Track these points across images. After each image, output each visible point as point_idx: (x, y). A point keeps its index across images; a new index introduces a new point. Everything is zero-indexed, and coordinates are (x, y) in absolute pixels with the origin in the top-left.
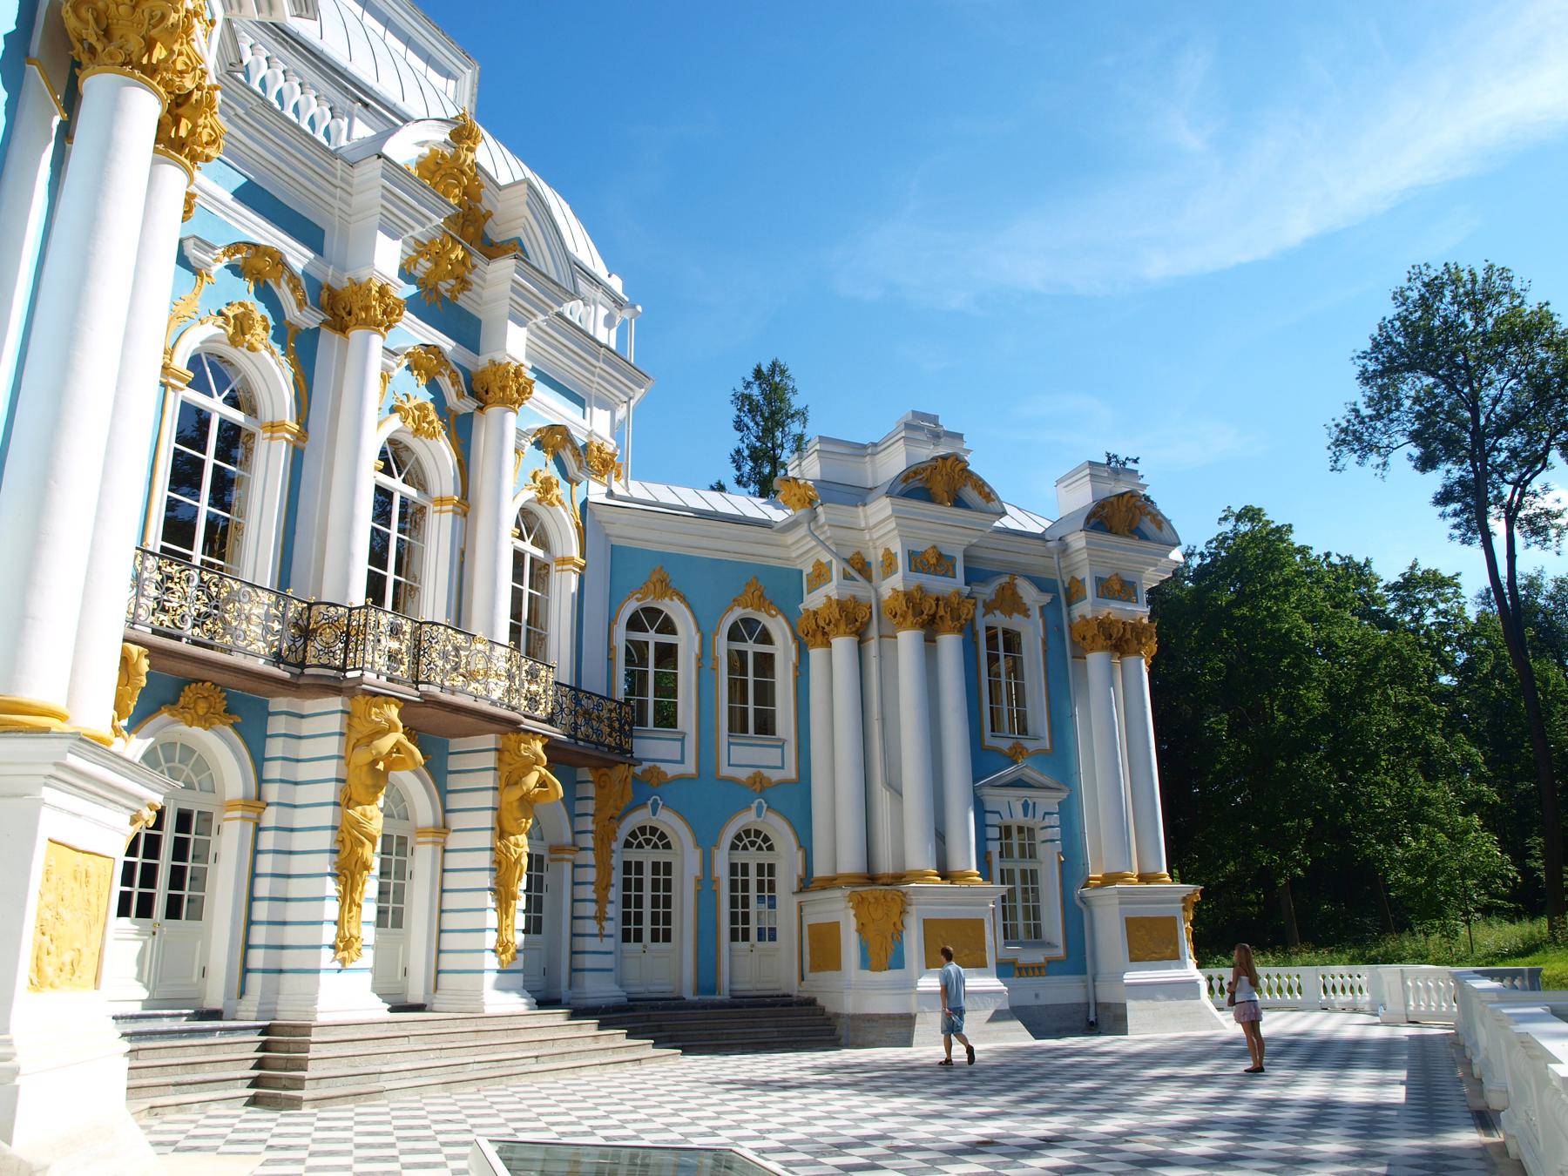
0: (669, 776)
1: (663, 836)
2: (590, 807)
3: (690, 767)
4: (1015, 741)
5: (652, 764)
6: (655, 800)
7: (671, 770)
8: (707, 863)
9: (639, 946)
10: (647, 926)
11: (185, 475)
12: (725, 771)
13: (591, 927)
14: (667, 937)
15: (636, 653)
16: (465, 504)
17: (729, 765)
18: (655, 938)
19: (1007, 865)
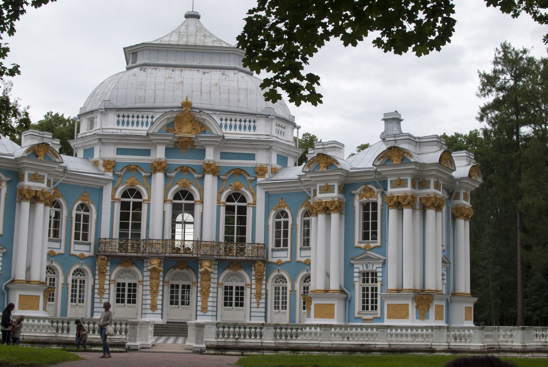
0: (283, 261)
1: (285, 279)
2: (253, 273)
3: (288, 259)
4: (367, 244)
5: (278, 259)
6: (278, 269)
7: (284, 260)
8: (293, 286)
9: (278, 311)
10: (280, 305)
11: (124, 216)
12: (299, 259)
13: (255, 305)
14: (286, 309)
15: (278, 225)
16: (202, 202)
17: (301, 257)
18: (282, 309)
19: (366, 285)
